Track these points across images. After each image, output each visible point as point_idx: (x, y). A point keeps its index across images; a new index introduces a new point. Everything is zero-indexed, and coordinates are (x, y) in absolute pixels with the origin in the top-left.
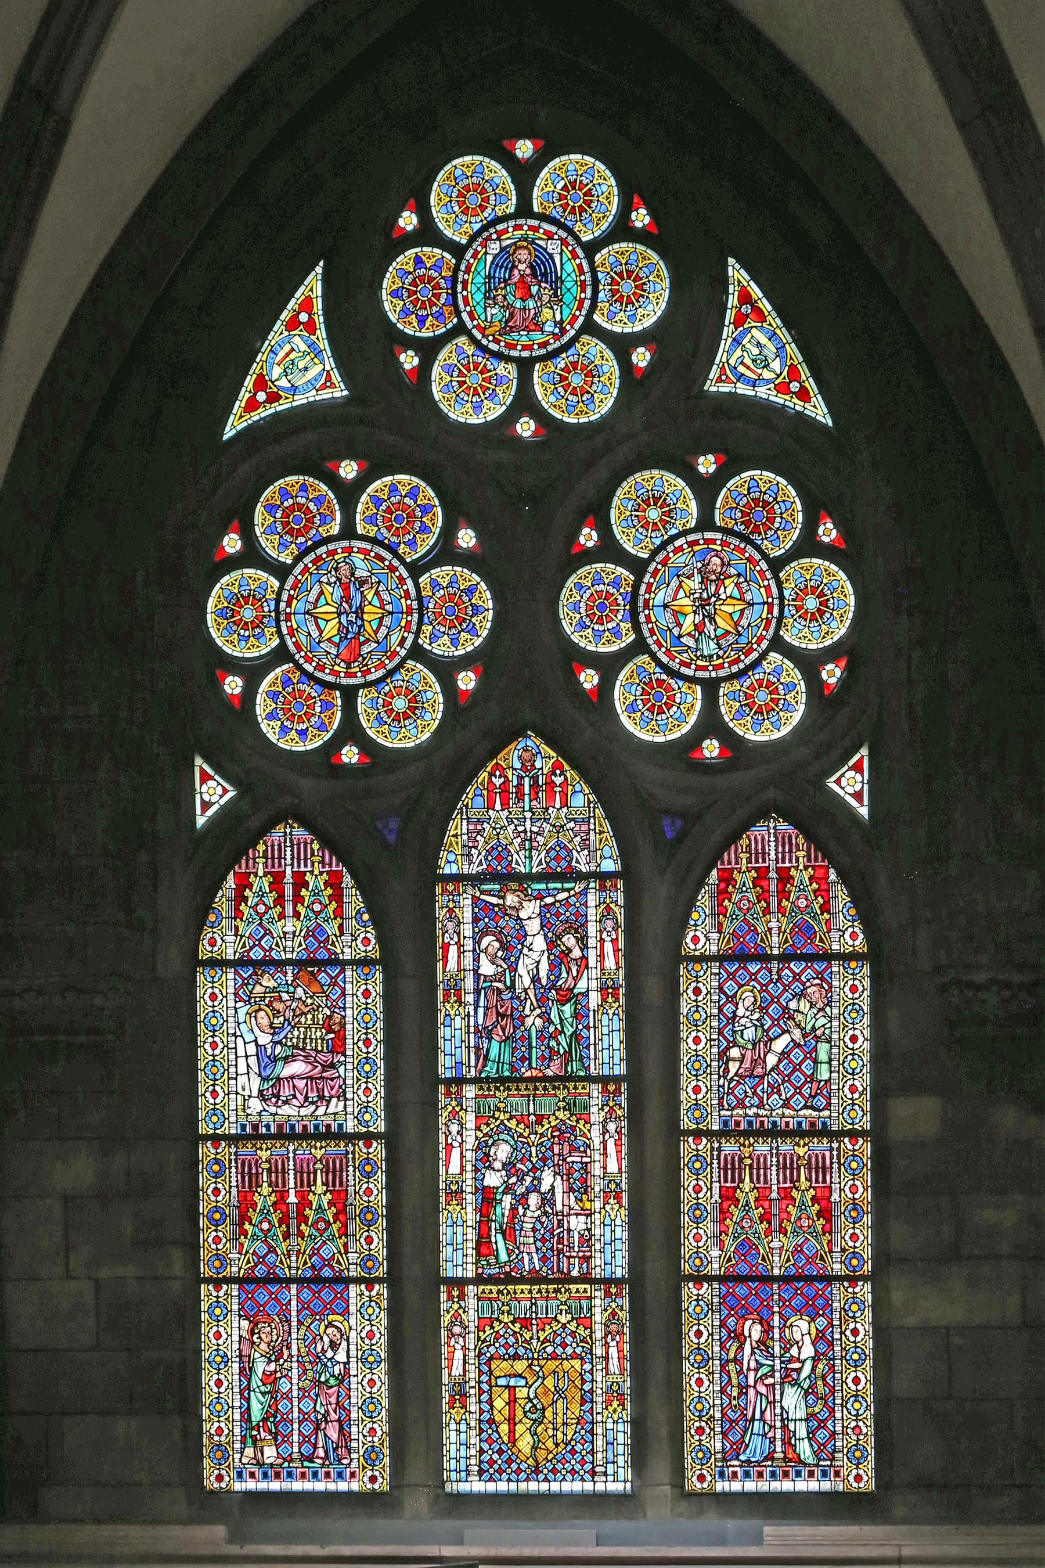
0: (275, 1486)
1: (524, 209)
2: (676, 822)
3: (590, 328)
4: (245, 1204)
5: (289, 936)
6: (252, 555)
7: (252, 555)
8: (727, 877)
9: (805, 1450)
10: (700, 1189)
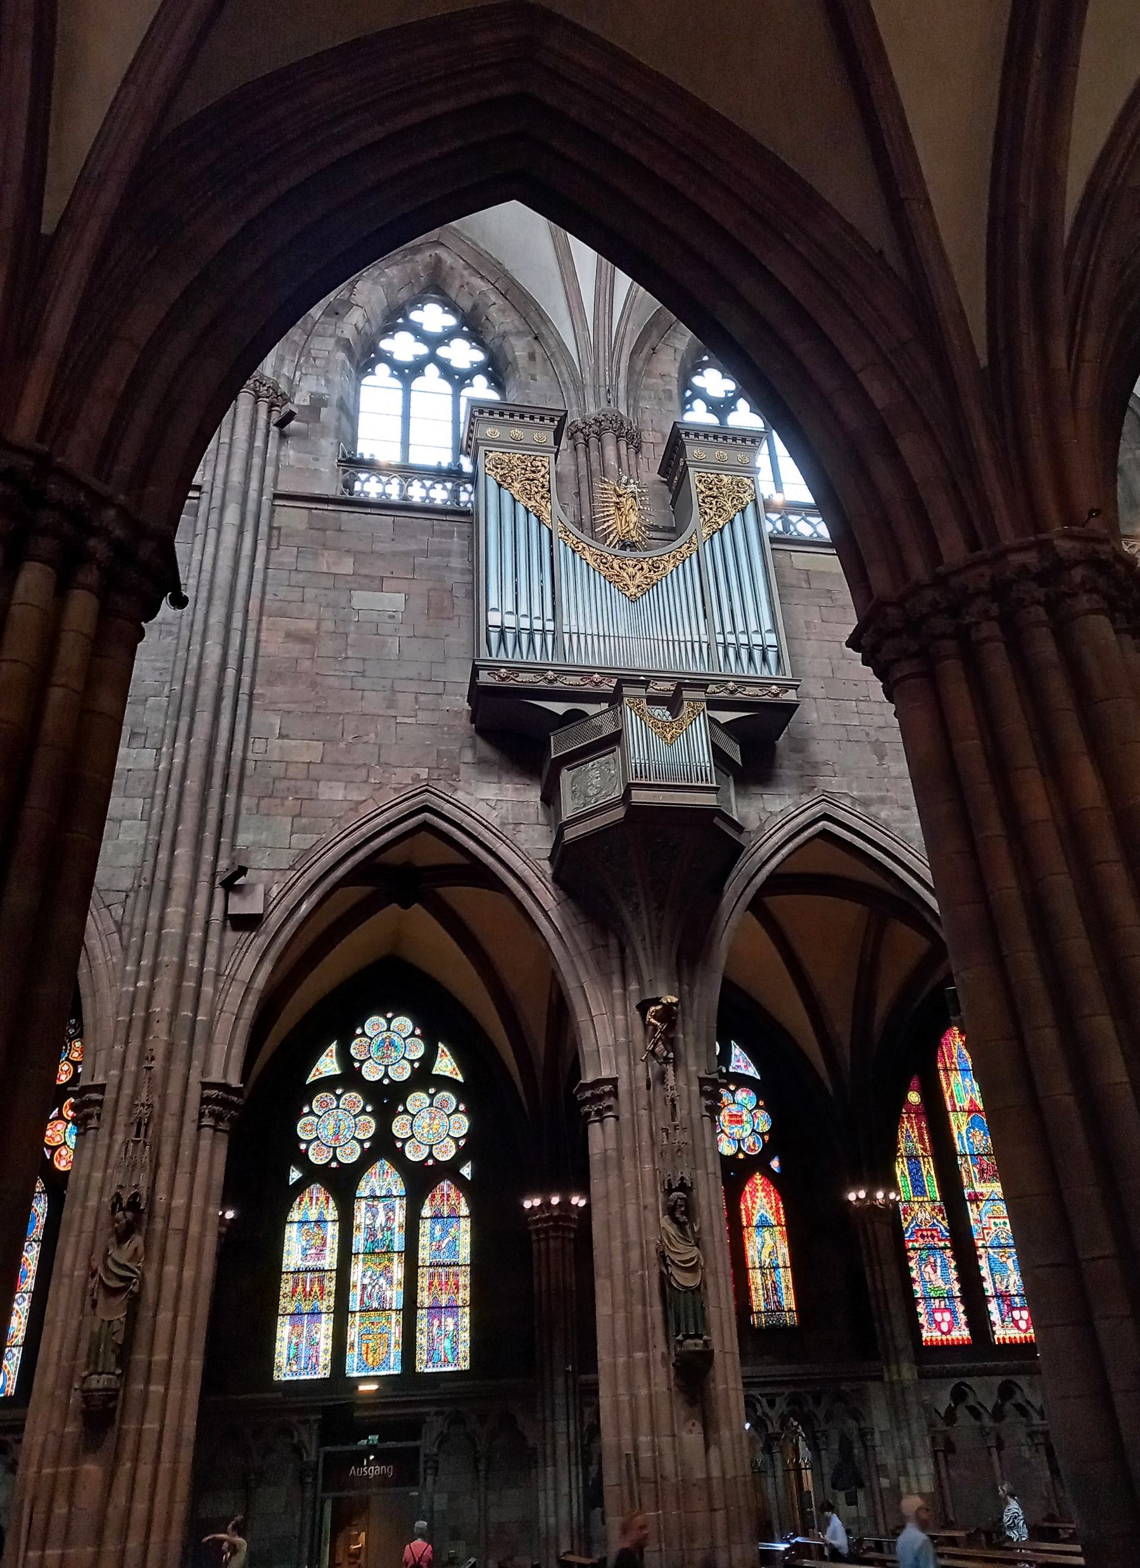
0: (295, 1378)
1: (388, 1030)
2: (420, 1180)
3: (404, 1058)
4: (294, 1292)
5: (313, 1215)
6: (311, 1112)
7: (311, 1112)
8: (433, 1196)
9: (450, 1358)
10: (423, 1282)
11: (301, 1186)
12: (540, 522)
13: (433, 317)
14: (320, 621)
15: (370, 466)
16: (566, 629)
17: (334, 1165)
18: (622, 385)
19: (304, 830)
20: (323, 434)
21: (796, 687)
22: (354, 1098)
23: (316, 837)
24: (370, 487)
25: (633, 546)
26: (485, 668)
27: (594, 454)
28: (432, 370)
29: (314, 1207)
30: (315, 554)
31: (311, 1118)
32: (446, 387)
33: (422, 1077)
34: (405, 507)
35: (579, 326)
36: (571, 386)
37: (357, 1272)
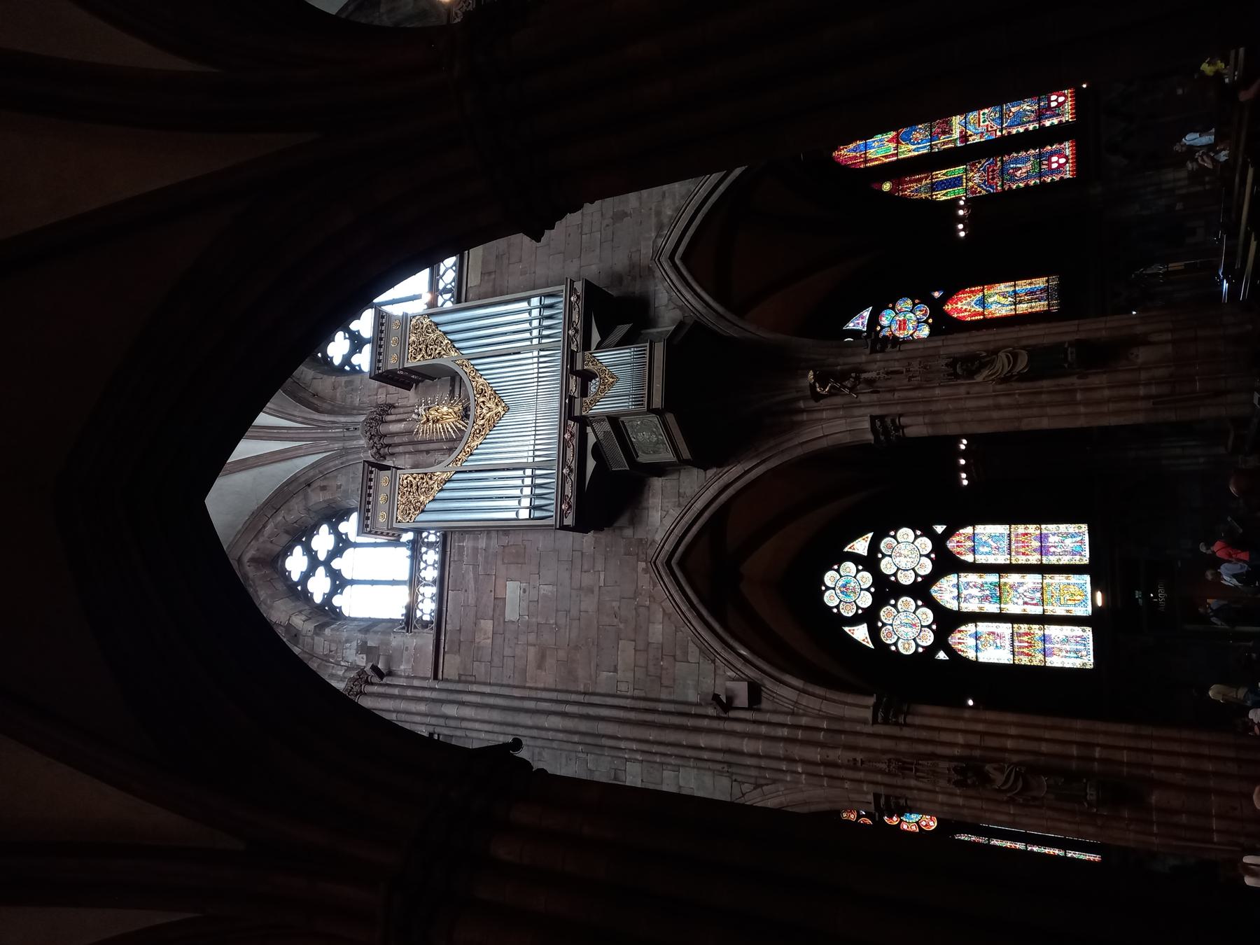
2: (946, 563)
4: (1028, 655)
5: (972, 642)
6: (895, 644)
7: (895, 644)
10: (1022, 560)
11: (950, 651)
12: (450, 481)
13: (296, 563)
14: (528, 644)
15: (411, 609)
16: (531, 460)
17: (934, 627)
18: (343, 419)
19: (686, 653)
20: (388, 644)
21: (572, 282)
22: (885, 614)
23: (691, 644)
24: (427, 609)
25: (466, 409)
26: (561, 520)
27: (397, 440)
28: (336, 564)
29: (965, 641)
30: (478, 648)
31: (900, 644)
32: (349, 552)
33: (870, 562)
34: (440, 582)
35: (301, 452)
36: (344, 459)
37: (1013, 608)
